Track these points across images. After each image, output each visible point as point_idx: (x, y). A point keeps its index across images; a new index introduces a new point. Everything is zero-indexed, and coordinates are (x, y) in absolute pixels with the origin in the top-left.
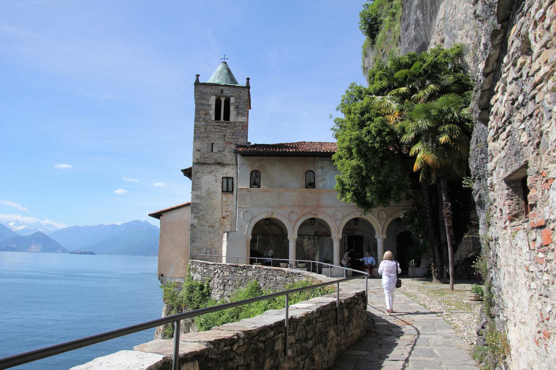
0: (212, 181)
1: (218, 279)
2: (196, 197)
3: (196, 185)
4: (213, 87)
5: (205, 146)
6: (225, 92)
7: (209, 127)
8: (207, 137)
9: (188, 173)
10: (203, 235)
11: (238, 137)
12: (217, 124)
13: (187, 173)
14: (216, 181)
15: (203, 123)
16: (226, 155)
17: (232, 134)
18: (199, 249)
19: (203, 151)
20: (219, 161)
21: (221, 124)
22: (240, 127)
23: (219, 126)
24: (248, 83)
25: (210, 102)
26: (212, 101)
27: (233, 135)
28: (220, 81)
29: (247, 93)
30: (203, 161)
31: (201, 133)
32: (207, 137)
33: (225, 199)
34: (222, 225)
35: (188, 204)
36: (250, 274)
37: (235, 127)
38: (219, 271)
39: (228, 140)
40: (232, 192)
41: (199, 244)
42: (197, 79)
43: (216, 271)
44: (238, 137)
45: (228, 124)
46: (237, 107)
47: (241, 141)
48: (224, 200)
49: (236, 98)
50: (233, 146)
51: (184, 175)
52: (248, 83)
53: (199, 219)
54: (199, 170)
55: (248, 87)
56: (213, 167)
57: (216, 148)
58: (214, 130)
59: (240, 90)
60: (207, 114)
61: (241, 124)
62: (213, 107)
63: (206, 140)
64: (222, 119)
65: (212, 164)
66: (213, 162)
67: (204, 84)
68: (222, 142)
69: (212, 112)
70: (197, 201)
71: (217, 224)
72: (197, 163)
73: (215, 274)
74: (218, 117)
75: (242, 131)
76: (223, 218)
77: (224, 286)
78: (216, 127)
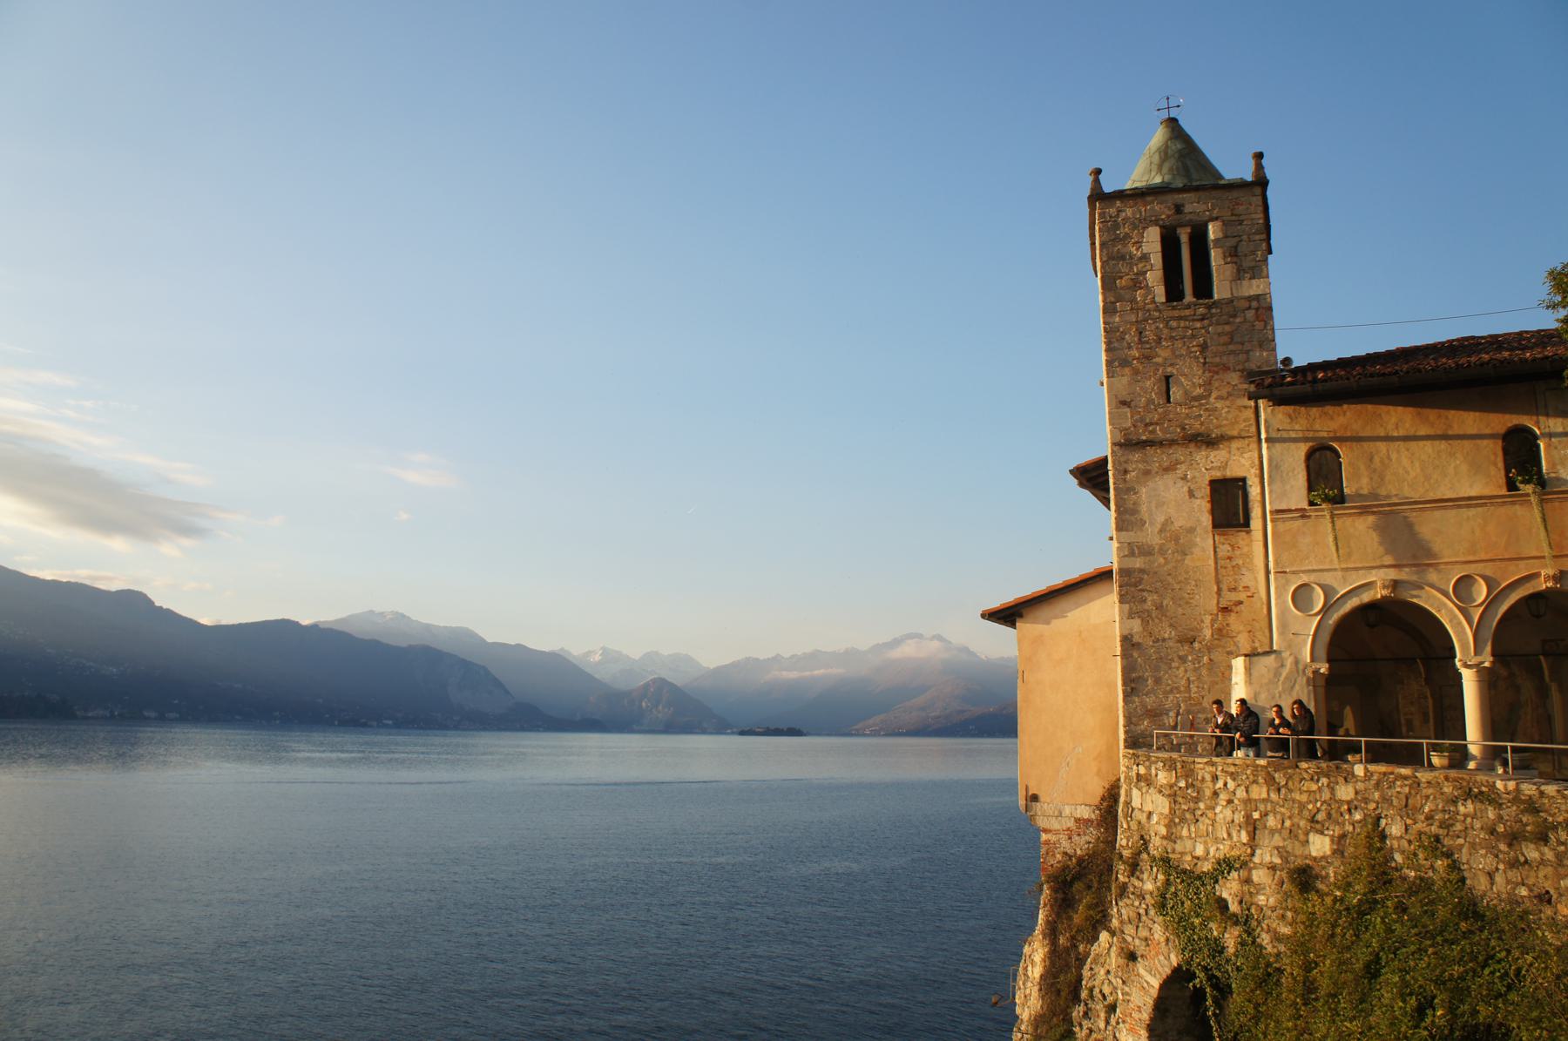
0: (1175, 499)
2: (1130, 550)
3: (1126, 511)
4: (1149, 199)
6: (1188, 209)
9: (1092, 476)
10: (1163, 666)
11: (1247, 346)
12: (1176, 313)
13: (1089, 480)
14: (1191, 494)
16: (1215, 409)
17: (1225, 339)
18: (1155, 714)
20: (1196, 427)
21: (1187, 312)
22: (1250, 314)
23: (1180, 318)
24: (1259, 167)
25: (1145, 249)
26: (1152, 241)
28: (1167, 178)
29: (1259, 200)
33: (1224, 550)
34: (1221, 633)
35: (1104, 576)
36: (1345, 792)
37: (1235, 316)
38: (1231, 785)
39: (1217, 360)
40: (1247, 524)
41: (1150, 701)
42: (1097, 182)
43: (1220, 784)
44: (1247, 346)
45: (1209, 307)
46: (1233, 254)
47: (1258, 358)
48: (1220, 554)
49: (1225, 224)
51: (1081, 485)
52: (1259, 167)
53: (1145, 618)
55: (1261, 183)
56: (1179, 453)
59: (1235, 194)
60: (1138, 283)
61: (1254, 304)
62: (1156, 259)
64: (1189, 298)
65: (1172, 443)
67: (1120, 195)
69: (1154, 277)
70: (1138, 563)
71: (1207, 633)
72: (1127, 443)
73: (1216, 794)
74: (1174, 292)
76: (1225, 610)
77: (1253, 836)
78: (1173, 324)
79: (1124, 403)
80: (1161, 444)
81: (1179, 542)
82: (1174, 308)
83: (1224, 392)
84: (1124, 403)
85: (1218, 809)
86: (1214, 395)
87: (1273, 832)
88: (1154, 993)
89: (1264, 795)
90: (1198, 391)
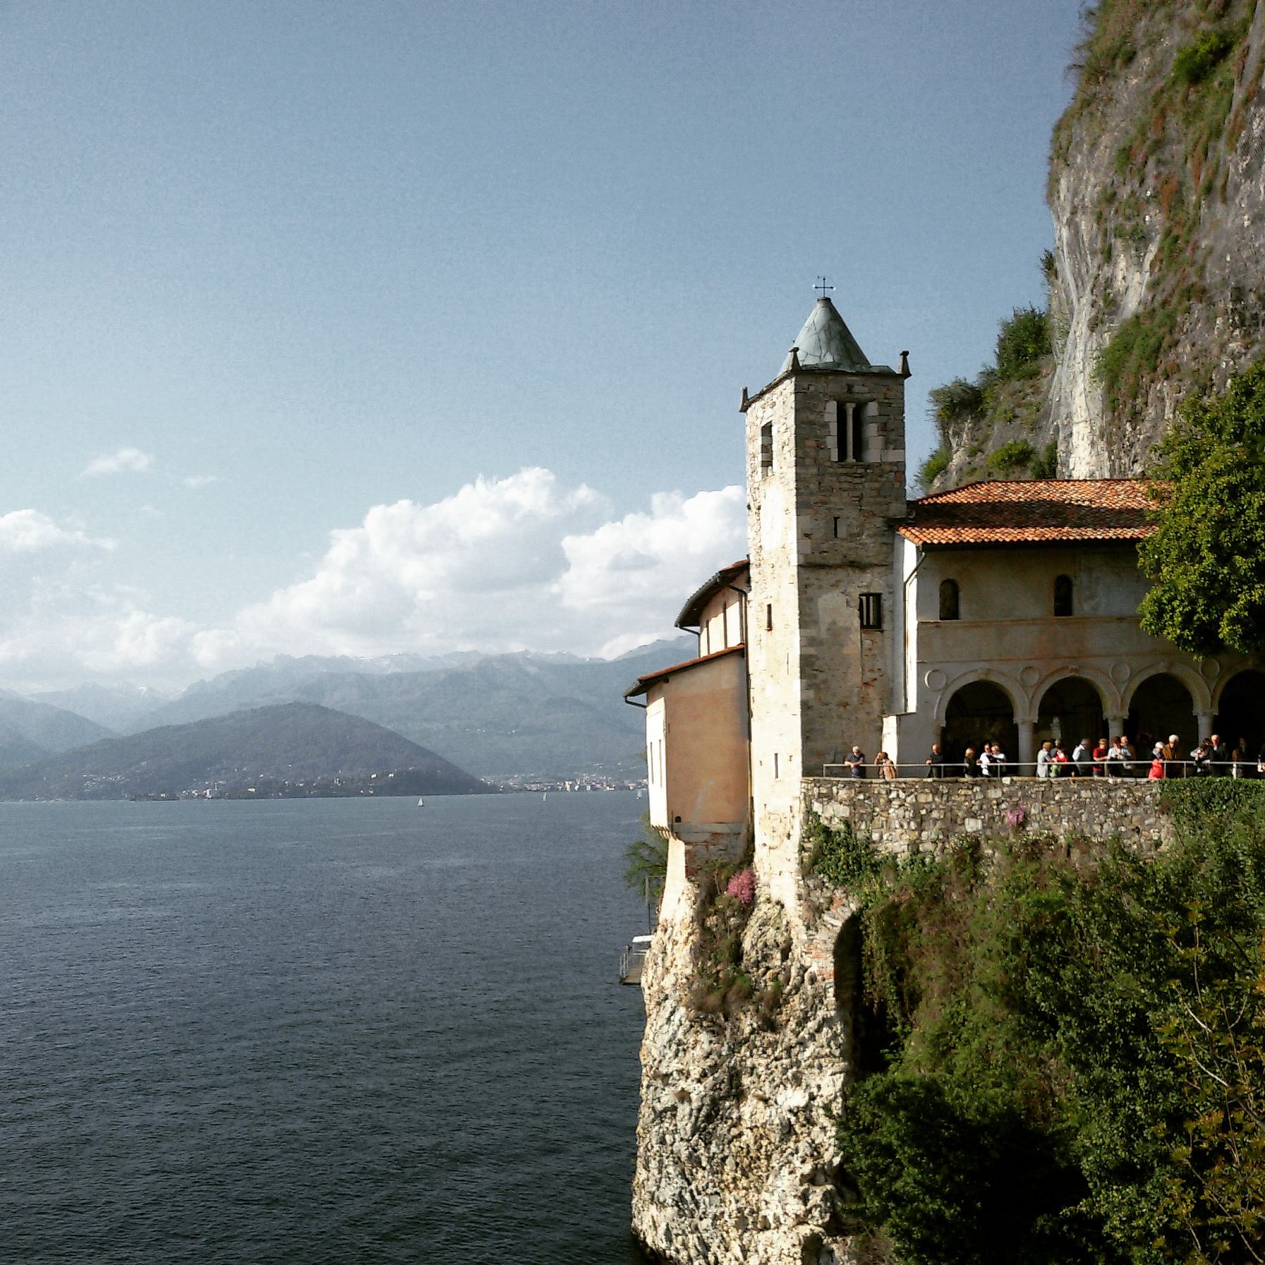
1: (901, 812)
5: (822, 524)
7: (827, 479)
8: (824, 503)
11: (888, 500)
12: (844, 471)
15: (814, 471)
19: (818, 535)
27: (879, 495)
30: (818, 559)
31: (812, 494)
32: (824, 503)
37: (881, 476)
43: (893, 795)
44: (888, 500)
50: (878, 522)
54: (812, 581)
56: (840, 574)
57: (844, 528)
58: (837, 485)
60: (820, 447)
63: (823, 509)
66: (838, 562)
68: (855, 514)
69: (832, 442)
73: (890, 801)
75: (897, 485)
78: (843, 478)
79: (807, 535)
80: (830, 567)
81: (837, 635)
82: (843, 467)
83: (871, 532)
84: (807, 535)
85: (891, 811)
86: (866, 533)
87: (936, 820)
88: (838, 930)
89: (930, 799)
90: (856, 531)
